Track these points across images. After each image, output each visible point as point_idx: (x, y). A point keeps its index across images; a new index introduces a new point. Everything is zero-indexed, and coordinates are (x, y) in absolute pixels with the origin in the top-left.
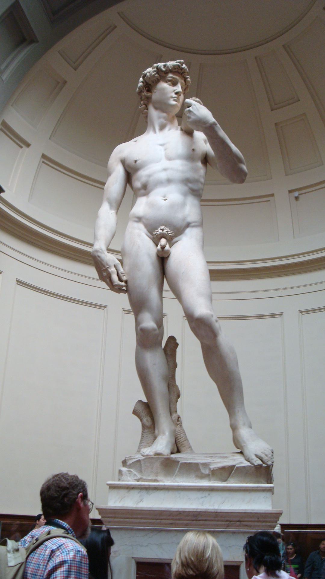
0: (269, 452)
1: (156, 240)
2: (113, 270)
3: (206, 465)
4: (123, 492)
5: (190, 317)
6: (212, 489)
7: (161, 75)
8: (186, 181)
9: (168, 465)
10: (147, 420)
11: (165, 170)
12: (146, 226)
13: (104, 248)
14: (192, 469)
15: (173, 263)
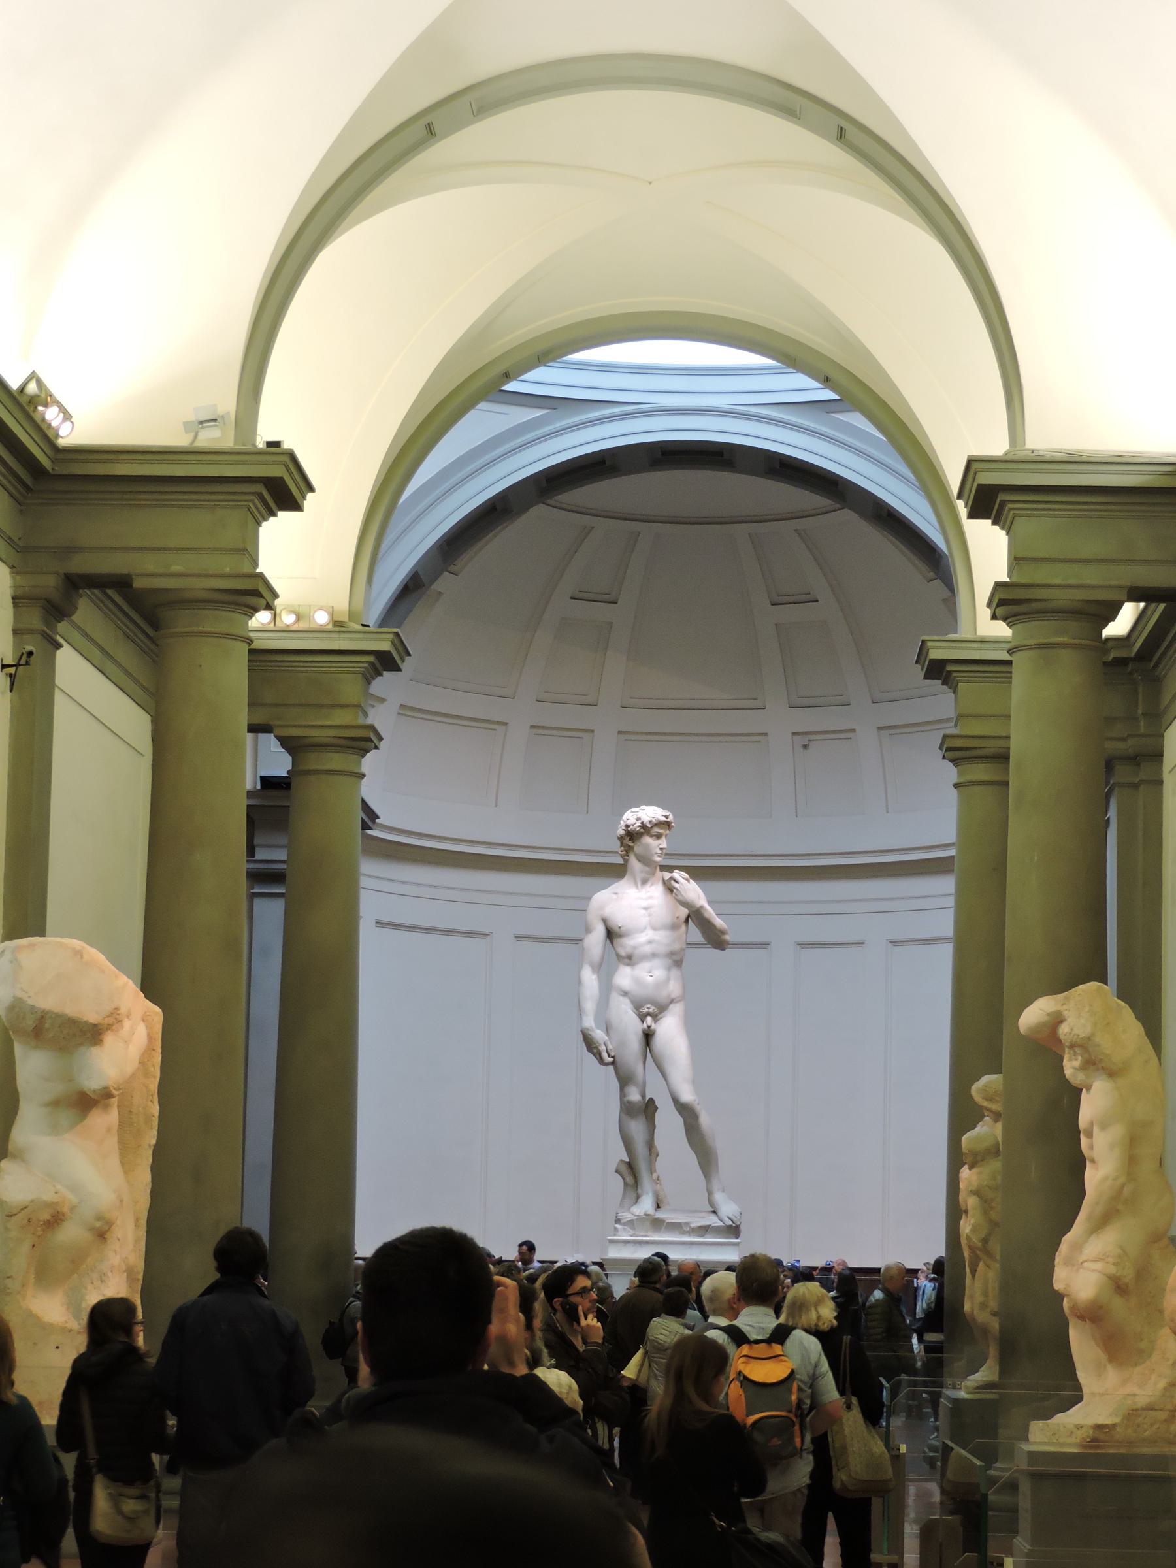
0: (738, 1214)
1: (642, 1018)
2: (603, 1048)
3: (687, 1224)
4: (620, 1245)
5: (676, 1101)
6: (692, 1243)
7: (646, 829)
8: (671, 954)
9: (657, 1224)
10: (630, 1179)
11: (650, 942)
12: (632, 1002)
13: (593, 1025)
14: (676, 1227)
15: (658, 1041)
